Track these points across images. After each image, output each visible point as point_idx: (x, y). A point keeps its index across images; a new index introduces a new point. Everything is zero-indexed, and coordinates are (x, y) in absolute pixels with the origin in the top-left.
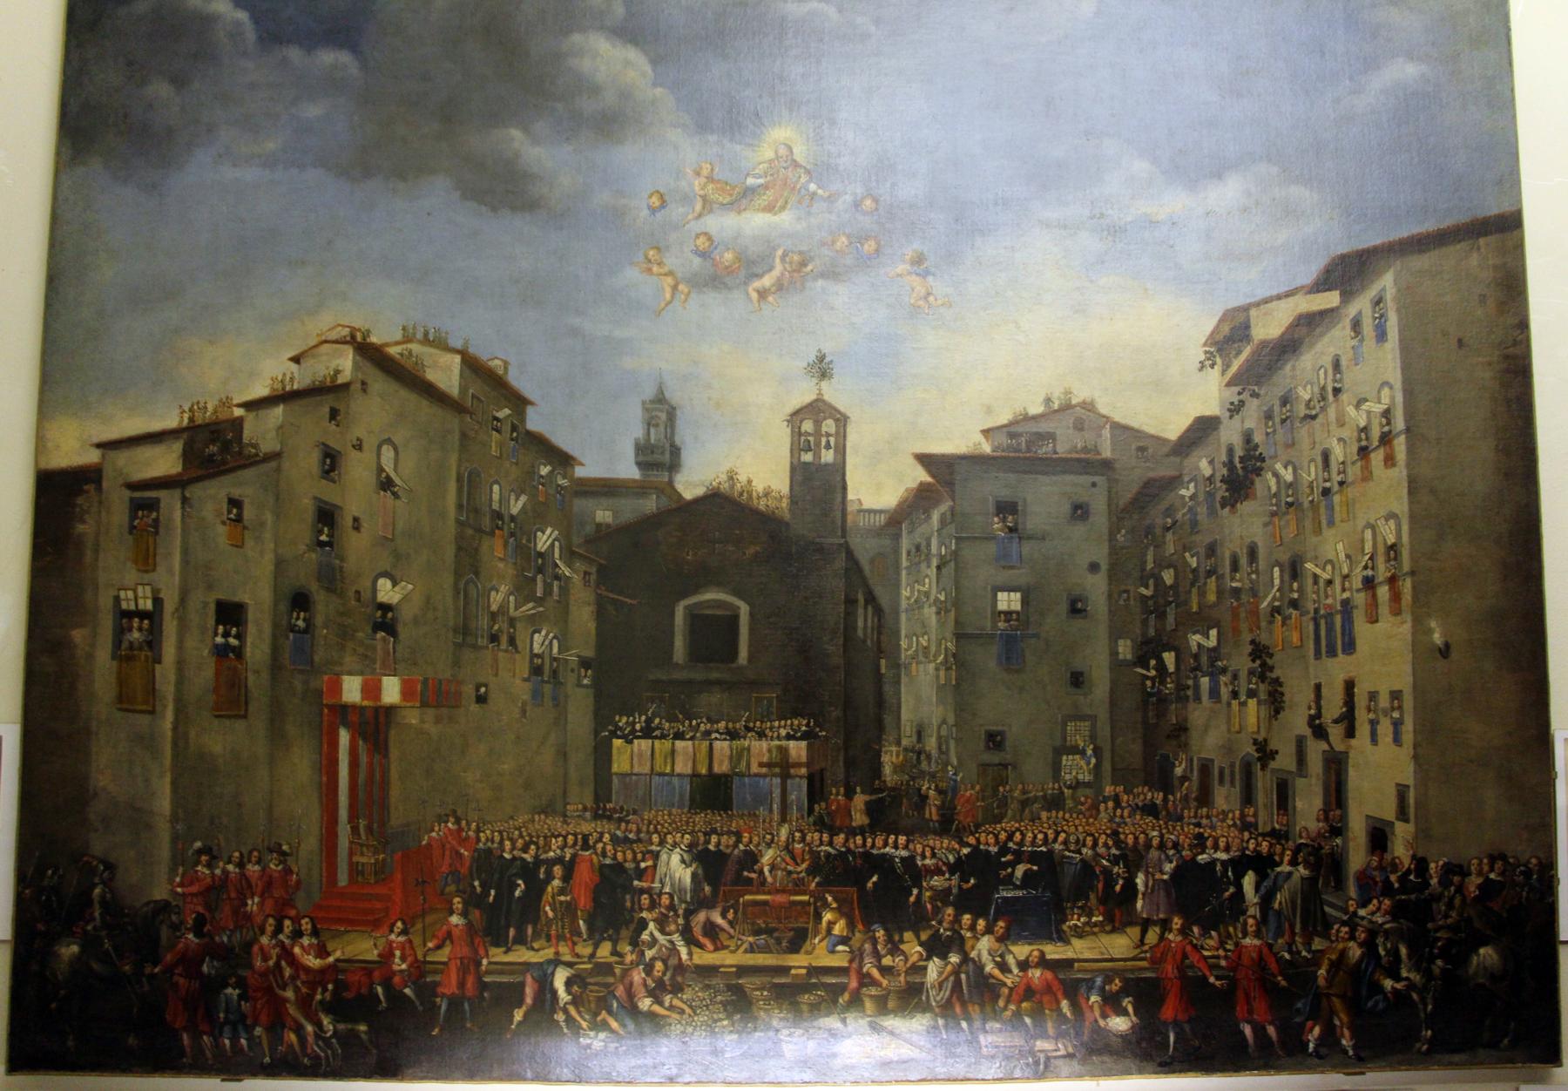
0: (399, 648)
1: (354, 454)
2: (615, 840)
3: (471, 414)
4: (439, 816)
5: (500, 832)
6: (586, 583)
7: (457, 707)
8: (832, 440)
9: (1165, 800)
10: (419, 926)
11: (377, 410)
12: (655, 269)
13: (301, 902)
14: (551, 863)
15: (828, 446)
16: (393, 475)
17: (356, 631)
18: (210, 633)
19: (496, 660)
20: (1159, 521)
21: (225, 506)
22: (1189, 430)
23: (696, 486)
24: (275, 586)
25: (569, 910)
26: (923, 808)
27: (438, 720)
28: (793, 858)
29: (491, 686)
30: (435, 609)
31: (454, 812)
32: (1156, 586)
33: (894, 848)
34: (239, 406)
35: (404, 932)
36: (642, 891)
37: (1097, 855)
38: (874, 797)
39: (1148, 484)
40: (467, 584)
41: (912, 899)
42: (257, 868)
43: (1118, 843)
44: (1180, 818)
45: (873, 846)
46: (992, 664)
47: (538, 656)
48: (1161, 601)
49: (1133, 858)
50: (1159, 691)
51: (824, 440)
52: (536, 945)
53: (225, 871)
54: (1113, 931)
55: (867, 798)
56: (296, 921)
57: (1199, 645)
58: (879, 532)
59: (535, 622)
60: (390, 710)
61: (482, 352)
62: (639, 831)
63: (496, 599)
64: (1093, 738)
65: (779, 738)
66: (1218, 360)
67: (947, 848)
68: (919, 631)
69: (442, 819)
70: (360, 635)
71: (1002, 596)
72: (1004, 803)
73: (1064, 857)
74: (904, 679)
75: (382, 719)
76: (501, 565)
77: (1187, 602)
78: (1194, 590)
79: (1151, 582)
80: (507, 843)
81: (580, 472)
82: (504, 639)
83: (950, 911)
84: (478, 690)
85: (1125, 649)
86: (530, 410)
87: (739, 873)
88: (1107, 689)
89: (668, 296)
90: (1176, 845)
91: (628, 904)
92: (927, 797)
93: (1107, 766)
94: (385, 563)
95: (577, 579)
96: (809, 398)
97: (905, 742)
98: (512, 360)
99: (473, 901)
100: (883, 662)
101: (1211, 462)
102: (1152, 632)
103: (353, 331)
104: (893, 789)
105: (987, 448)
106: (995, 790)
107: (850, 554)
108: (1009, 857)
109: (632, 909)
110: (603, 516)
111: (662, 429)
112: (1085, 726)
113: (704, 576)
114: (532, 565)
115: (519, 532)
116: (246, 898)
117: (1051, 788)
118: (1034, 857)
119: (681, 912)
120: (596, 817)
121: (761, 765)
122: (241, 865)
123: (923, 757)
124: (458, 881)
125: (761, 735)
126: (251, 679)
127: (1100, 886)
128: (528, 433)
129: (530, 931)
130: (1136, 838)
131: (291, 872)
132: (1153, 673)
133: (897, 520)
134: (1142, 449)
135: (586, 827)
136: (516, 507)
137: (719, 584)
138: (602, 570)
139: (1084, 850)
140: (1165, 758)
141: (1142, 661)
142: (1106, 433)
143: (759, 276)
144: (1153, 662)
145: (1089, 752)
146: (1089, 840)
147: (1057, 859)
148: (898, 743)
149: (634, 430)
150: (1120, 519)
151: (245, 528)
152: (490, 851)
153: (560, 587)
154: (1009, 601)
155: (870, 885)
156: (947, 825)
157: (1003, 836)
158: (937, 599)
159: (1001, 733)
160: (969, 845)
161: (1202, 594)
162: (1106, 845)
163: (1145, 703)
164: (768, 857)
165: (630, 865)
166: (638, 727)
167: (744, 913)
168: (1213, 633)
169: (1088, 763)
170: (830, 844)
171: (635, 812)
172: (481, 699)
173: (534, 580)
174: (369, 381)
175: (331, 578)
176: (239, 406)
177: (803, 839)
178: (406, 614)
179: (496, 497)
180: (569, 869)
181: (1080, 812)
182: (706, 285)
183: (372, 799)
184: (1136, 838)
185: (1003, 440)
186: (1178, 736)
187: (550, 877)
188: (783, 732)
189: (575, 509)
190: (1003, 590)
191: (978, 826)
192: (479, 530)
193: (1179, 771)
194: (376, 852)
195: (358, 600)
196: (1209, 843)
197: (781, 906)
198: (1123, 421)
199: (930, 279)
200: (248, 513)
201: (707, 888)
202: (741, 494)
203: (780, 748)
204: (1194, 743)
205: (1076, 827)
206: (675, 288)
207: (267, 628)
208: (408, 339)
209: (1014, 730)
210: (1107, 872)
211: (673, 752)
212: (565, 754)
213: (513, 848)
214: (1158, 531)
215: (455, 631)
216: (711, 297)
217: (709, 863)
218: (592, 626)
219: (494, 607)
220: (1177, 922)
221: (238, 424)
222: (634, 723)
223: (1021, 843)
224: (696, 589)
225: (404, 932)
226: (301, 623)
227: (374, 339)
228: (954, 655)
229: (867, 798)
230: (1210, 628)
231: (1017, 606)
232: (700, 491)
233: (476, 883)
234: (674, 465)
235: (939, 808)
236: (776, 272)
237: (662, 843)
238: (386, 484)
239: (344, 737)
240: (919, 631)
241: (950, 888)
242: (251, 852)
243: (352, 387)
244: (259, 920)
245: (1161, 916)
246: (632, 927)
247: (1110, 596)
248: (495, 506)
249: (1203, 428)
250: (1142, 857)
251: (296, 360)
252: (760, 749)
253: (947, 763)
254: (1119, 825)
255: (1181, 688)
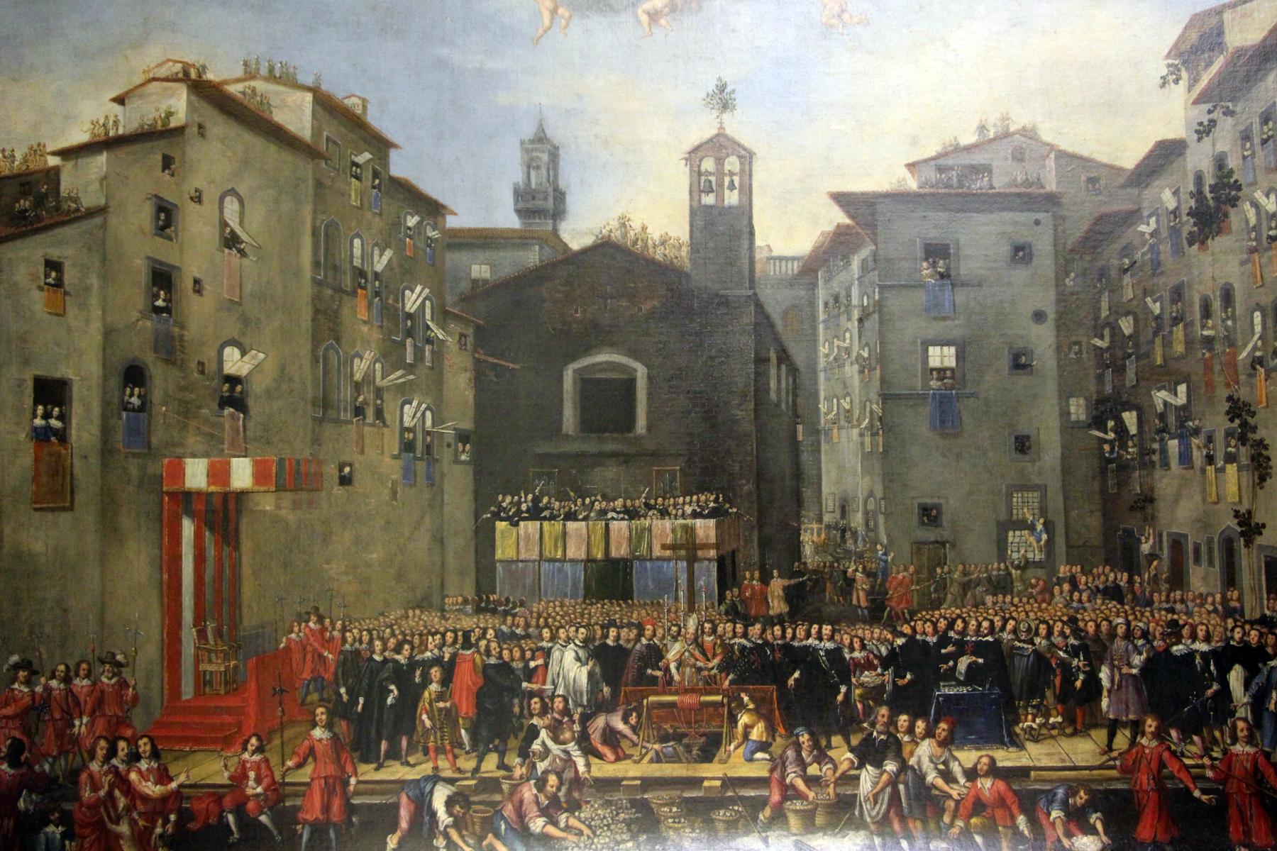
0: (251, 425)
1: (193, 206)
2: (500, 636)
3: (326, 159)
5: (369, 631)
7: (317, 490)
8: (736, 180)
9: (1131, 581)
10: (277, 742)
11: (216, 157)
13: (138, 719)
17: (199, 407)
18: (28, 414)
19: (362, 436)
20: (1115, 262)
21: (42, 269)
22: (1148, 157)
26: (851, 594)
27: (296, 505)
28: (704, 653)
29: (357, 465)
30: (291, 379)
31: (317, 609)
32: (1113, 336)
34: (54, 153)
35: (260, 749)
36: (532, 694)
37: (1053, 645)
38: (793, 582)
39: (1100, 219)
40: (326, 350)
41: (840, 698)
42: (86, 682)
43: (1077, 632)
44: (1149, 603)
46: (924, 429)
47: (408, 430)
49: (1094, 649)
50: (1120, 457)
51: (727, 180)
52: (412, 760)
53: (48, 689)
54: (1075, 733)
55: (786, 582)
56: (132, 741)
57: (1165, 403)
58: (792, 282)
60: (241, 495)
61: (336, 89)
62: (527, 625)
63: (360, 368)
64: (1043, 511)
65: (683, 516)
66: (1184, 74)
67: (878, 639)
68: (840, 391)
69: (303, 618)
70: (205, 412)
71: (934, 351)
72: (942, 586)
73: (1013, 647)
74: (824, 447)
75: (232, 506)
76: (365, 329)
78: (1158, 341)
79: (1107, 332)
80: (378, 644)
81: (452, 222)
82: (370, 412)
83: (884, 710)
84: (341, 470)
85: (1078, 409)
86: (394, 155)
88: (1059, 455)
89: (547, 22)
90: (1145, 634)
91: (517, 709)
92: (854, 580)
93: (1060, 541)
94: (232, 331)
98: (371, 97)
99: (339, 711)
100: (800, 428)
102: (1108, 389)
104: (815, 572)
105: (912, 184)
106: (932, 572)
107: (759, 306)
108: (950, 648)
109: (521, 714)
110: (480, 270)
112: (1033, 497)
114: (400, 330)
115: (383, 292)
116: (72, 719)
117: (996, 568)
118: (978, 649)
119: (576, 717)
120: (479, 610)
121: (664, 547)
122: (67, 680)
123: (848, 535)
125: (664, 513)
126: (77, 463)
127: (1058, 681)
129: (404, 743)
130: (1098, 626)
131: (128, 686)
132: (1111, 435)
133: (813, 267)
134: (1093, 181)
135: (467, 623)
137: (612, 345)
138: (478, 329)
139: (1037, 640)
140: (1129, 533)
141: (1098, 422)
142: (1051, 163)
144: (1111, 424)
145: (1039, 527)
146: (1043, 629)
147: (1005, 648)
148: (820, 520)
150: (1068, 262)
151: (66, 293)
152: (357, 653)
153: (433, 352)
154: (942, 356)
155: (791, 682)
156: (877, 612)
157: (942, 624)
158: (859, 355)
159: (938, 507)
160: (904, 635)
161: (1167, 343)
162: (1062, 633)
163: (1103, 471)
164: (674, 652)
165: (518, 665)
166: (524, 507)
167: (649, 717)
168: (1182, 388)
169: (1039, 540)
170: (745, 635)
171: (522, 604)
172: (345, 481)
174: (208, 124)
175: (170, 348)
176: (54, 153)
177: (714, 631)
178: (258, 387)
179: (357, 251)
180: (449, 670)
181: (1031, 596)
183: (220, 600)
184: (1098, 626)
185: (933, 175)
186: (1143, 508)
187: (426, 681)
188: (688, 509)
189: (448, 264)
190: (934, 344)
191: (913, 613)
192: (339, 290)
193: (1145, 548)
194: (226, 658)
195: (202, 372)
196: (1185, 631)
197: (691, 708)
198: (1070, 149)
200: (70, 276)
201: (606, 690)
202: (635, 243)
204: (1163, 514)
207: (96, 407)
208: (250, 75)
209: (952, 505)
210: (1065, 666)
211: (564, 534)
213: (384, 650)
214: (1114, 273)
215: (314, 404)
217: (608, 661)
218: (470, 395)
219: (358, 377)
220: (1151, 724)
222: (519, 503)
223: (964, 632)
224: (588, 350)
225: (260, 749)
226: (135, 401)
227: (210, 76)
228: (880, 419)
229: (786, 582)
230: (1177, 383)
231: (951, 362)
232: (588, 241)
233: (343, 690)
234: (558, 213)
235: (868, 593)
237: (554, 638)
238: (231, 241)
239: (188, 528)
240: (840, 391)
241: (883, 685)
242: (78, 665)
243: (188, 131)
244: (88, 743)
245: (1131, 717)
246: (522, 735)
247: (1058, 348)
249: (1166, 154)
250: (1105, 648)
251: (120, 100)
252: (663, 529)
253: (875, 542)
254: (1077, 611)
255: (1145, 452)
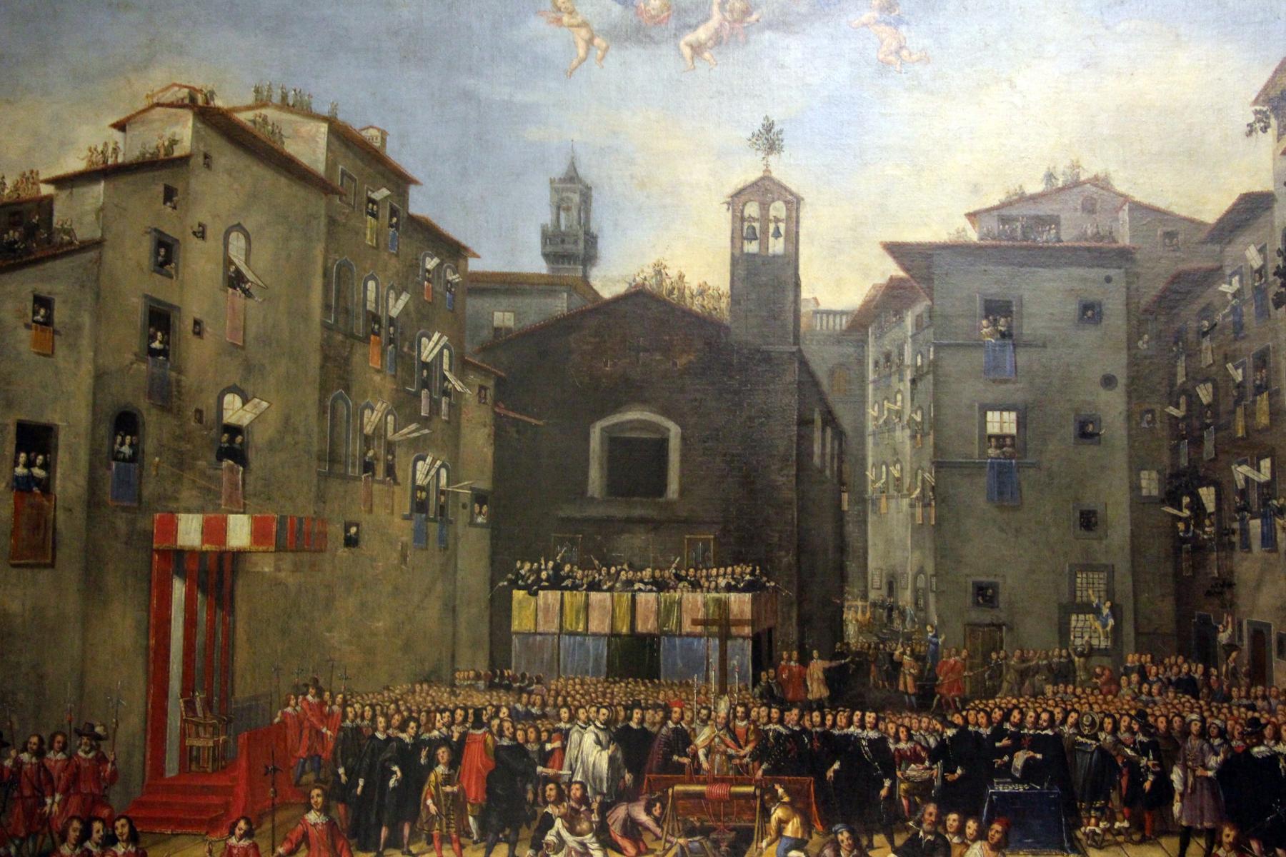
0: (251, 479)
1: (196, 243)
2: (515, 716)
3: (340, 194)
4: (296, 687)
5: (372, 706)
6: (481, 399)
7: (321, 551)
8: (782, 226)
9: (1206, 674)
10: (267, 826)
11: (222, 190)
12: (566, 19)
13: (117, 798)
14: (434, 744)
15: (777, 234)
16: (244, 269)
17: (195, 458)
18: (9, 462)
19: (370, 494)
20: (1193, 324)
21: (30, 305)
22: (1231, 211)
23: (615, 282)
24: (94, 405)
25: (456, 804)
26: (897, 679)
27: (297, 568)
28: (735, 739)
29: (364, 525)
30: (296, 431)
31: (316, 681)
32: (1189, 405)
33: (861, 727)
34: (47, 182)
35: (248, 834)
36: (547, 780)
37: (1118, 742)
38: (834, 664)
39: (1177, 278)
40: (335, 400)
41: (883, 792)
42: (60, 756)
43: (1146, 728)
44: (1228, 698)
45: (834, 724)
46: (981, 501)
47: (422, 488)
48: (1196, 424)
49: (1166, 747)
50: (1195, 536)
51: (772, 227)
52: (414, 849)
53: (18, 763)
54: (1142, 841)
55: (827, 664)
56: (109, 823)
57: (1247, 479)
58: (839, 338)
59: (418, 448)
60: (238, 554)
61: (354, 119)
62: (544, 704)
63: (371, 420)
64: (1110, 594)
65: (717, 589)
66: (1273, 122)
67: (926, 729)
68: (890, 459)
69: (300, 690)
70: (201, 464)
71: (993, 417)
72: (997, 673)
73: (1075, 743)
74: (871, 518)
75: (227, 567)
76: (377, 378)
77: (1229, 426)
78: (1240, 411)
79: (1183, 400)
80: (381, 721)
81: (474, 265)
82: (380, 469)
83: (931, 808)
84: (347, 530)
85: (1150, 483)
86: (413, 191)
87: (667, 758)
88: (1128, 532)
89: (581, 52)
90: (1222, 733)
91: (530, 796)
92: (900, 664)
93: (1128, 628)
94: (234, 378)
95: (470, 394)
96: (754, 175)
97: (873, 595)
98: (392, 130)
99: (337, 793)
100: (845, 496)
101: (1261, 251)
102: (1184, 462)
103: (193, 93)
104: (858, 654)
105: (973, 236)
106: (986, 656)
107: (804, 363)
108: (1006, 742)
109: (535, 802)
110: (503, 318)
111: (574, 212)
112: (1099, 578)
113: (627, 391)
114: (415, 380)
115: (399, 339)
116: (44, 796)
117: (1057, 655)
118: (1037, 743)
119: (595, 806)
120: (491, 686)
121: (695, 622)
122: (40, 753)
123: (895, 614)
124: (317, 769)
125: (696, 585)
126: (61, 516)
127: (1124, 782)
128: (413, 219)
129: (406, 831)
130: (1169, 722)
131: (106, 761)
132: (1186, 513)
133: (863, 322)
134: (1170, 235)
135: (479, 700)
136: (396, 307)
137: (644, 402)
138: (500, 382)
139: (1102, 736)
140: (1205, 621)
141: (1172, 498)
142: (1124, 215)
143: (693, 28)
144: (1186, 500)
145: (1106, 611)
146: (1108, 723)
147: (1066, 744)
148: (865, 597)
149: (537, 213)
150: (1140, 323)
151: (55, 332)
152: (358, 729)
153: (450, 405)
154: (1002, 422)
155: (830, 774)
156: (926, 699)
157: (997, 714)
158: (911, 418)
159: (994, 586)
160: (955, 726)
161: (1250, 414)
162: (1129, 729)
163: (1177, 551)
164: (703, 737)
165: (532, 747)
166: (544, 575)
167: (674, 808)
168: (1266, 464)
169: (1104, 626)
170: (781, 721)
171: (539, 681)
172: (351, 542)
173: (417, 396)
174: (214, 155)
175: (166, 394)
176: (47, 182)
177: (747, 715)
178: (260, 437)
179: (371, 295)
180: (458, 750)
181: (1095, 687)
182: (627, 39)
183: (212, 667)
184: (1169, 722)
185: (993, 224)
186: (1221, 593)
187: (433, 762)
188: (722, 582)
189: (469, 310)
190: (993, 409)
191: (965, 702)
192: (350, 335)
193: (1223, 637)
194: (216, 733)
195: (200, 421)
196: (1268, 731)
197: (720, 799)
198: (1146, 201)
199: (903, 29)
200: (61, 314)
201: (628, 777)
202: (671, 292)
203: (718, 602)
204: (1243, 603)
205: (1090, 705)
206: (590, 42)
207: (83, 456)
208: (261, 103)
209: (1010, 583)
210: (1132, 765)
211: (587, 606)
212: (454, 610)
213: (388, 726)
214: (1191, 336)
215: (320, 459)
216: (634, 53)
217: (631, 745)
218: (489, 452)
219: (368, 430)
220: (1228, 834)
221: (46, 205)
222: (539, 571)
223: (1020, 725)
224: (617, 407)
225: (248, 834)
226: (126, 449)
227: (219, 103)
228: (933, 489)
229: (827, 664)
230: (1260, 458)
231: (1011, 429)
232: (621, 289)
233: (341, 771)
234: (589, 257)
235: (916, 679)
236: (714, 23)
237: (572, 719)
238: (236, 280)
239: (179, 589)
240: (890, 459)
241: (930, 780)
242: (53, 737)
243: (192, 161)
244: (59, 823)
245: (1207, 824)
246: (535, 825)
247: (1129, 417)
248: (371, 306)
249: (1252, 208)
250: (1177, 747)
251: (121, 126)
252: (694, 602)
253: (925, 623)
254: (1146, 704)
255: (1224, 532)
